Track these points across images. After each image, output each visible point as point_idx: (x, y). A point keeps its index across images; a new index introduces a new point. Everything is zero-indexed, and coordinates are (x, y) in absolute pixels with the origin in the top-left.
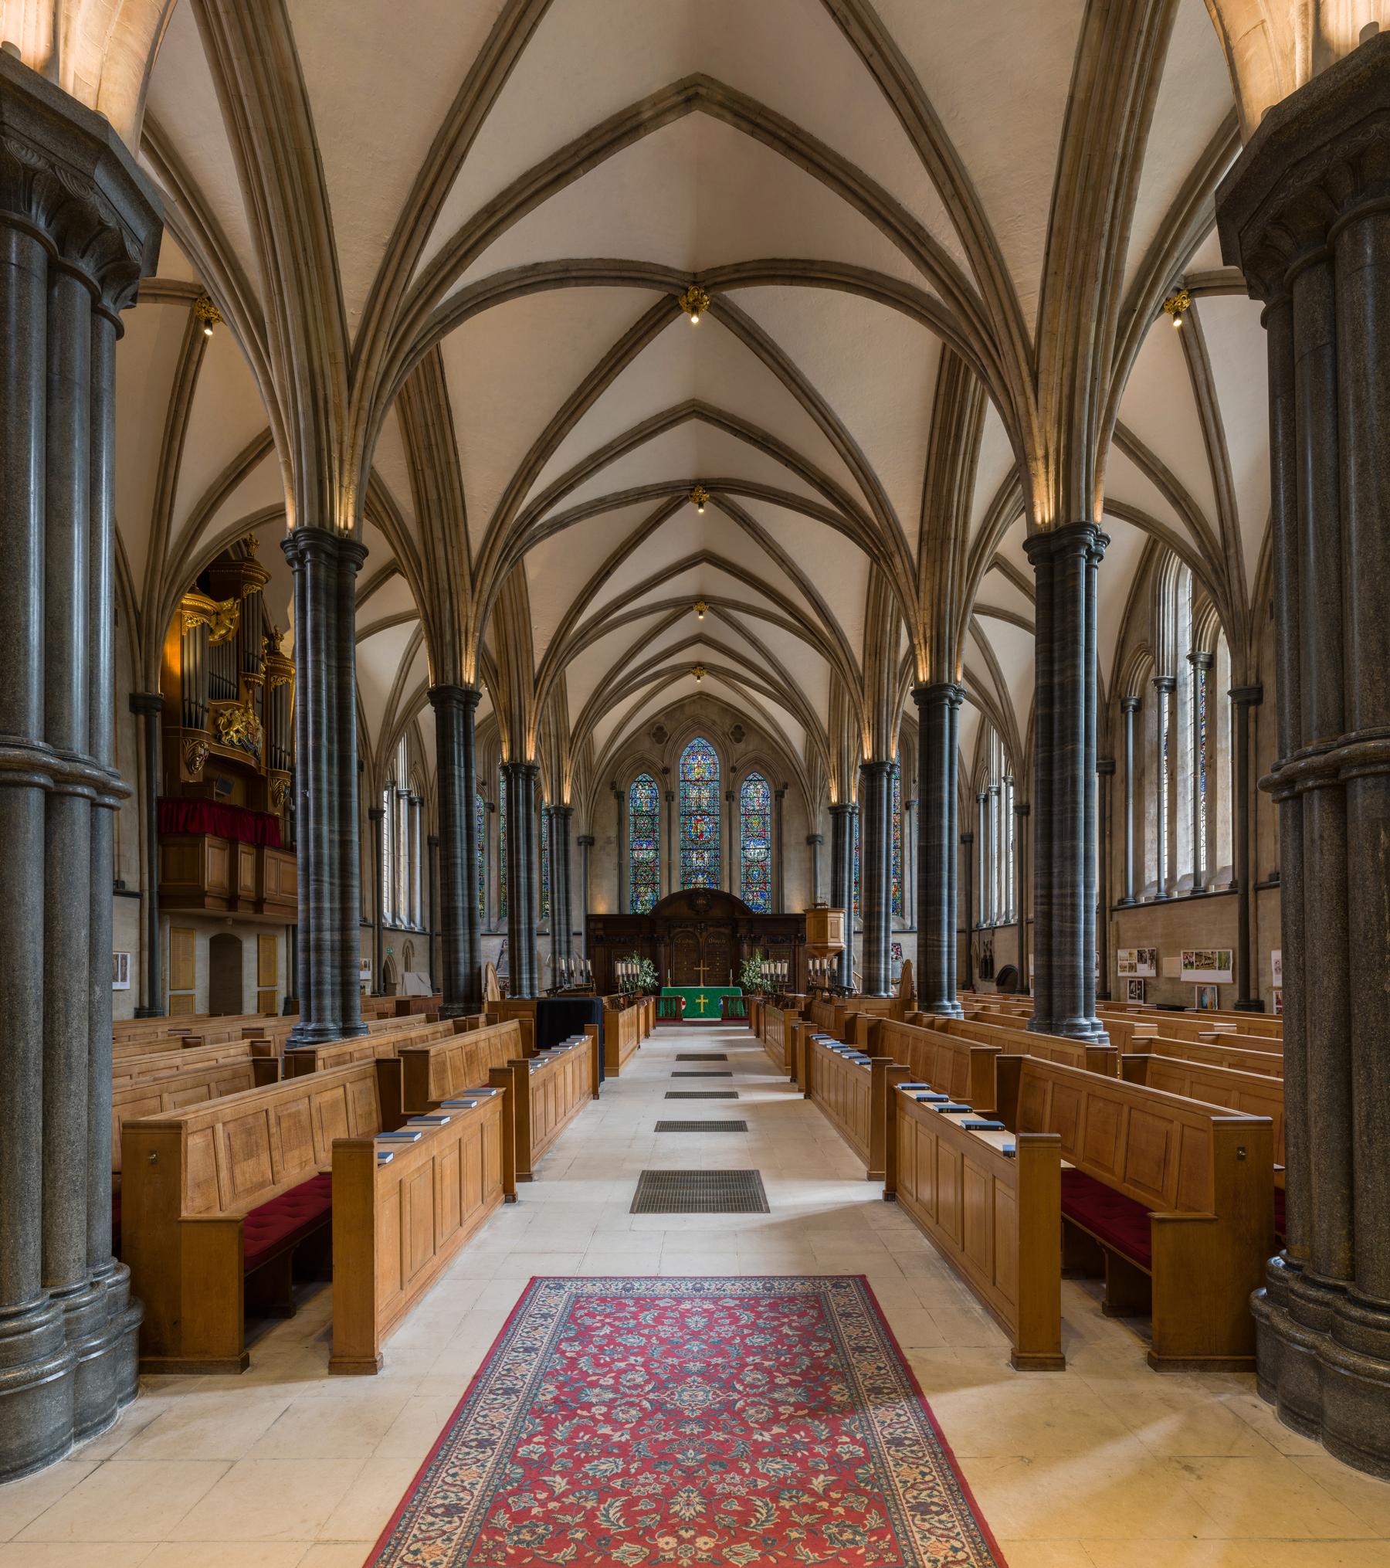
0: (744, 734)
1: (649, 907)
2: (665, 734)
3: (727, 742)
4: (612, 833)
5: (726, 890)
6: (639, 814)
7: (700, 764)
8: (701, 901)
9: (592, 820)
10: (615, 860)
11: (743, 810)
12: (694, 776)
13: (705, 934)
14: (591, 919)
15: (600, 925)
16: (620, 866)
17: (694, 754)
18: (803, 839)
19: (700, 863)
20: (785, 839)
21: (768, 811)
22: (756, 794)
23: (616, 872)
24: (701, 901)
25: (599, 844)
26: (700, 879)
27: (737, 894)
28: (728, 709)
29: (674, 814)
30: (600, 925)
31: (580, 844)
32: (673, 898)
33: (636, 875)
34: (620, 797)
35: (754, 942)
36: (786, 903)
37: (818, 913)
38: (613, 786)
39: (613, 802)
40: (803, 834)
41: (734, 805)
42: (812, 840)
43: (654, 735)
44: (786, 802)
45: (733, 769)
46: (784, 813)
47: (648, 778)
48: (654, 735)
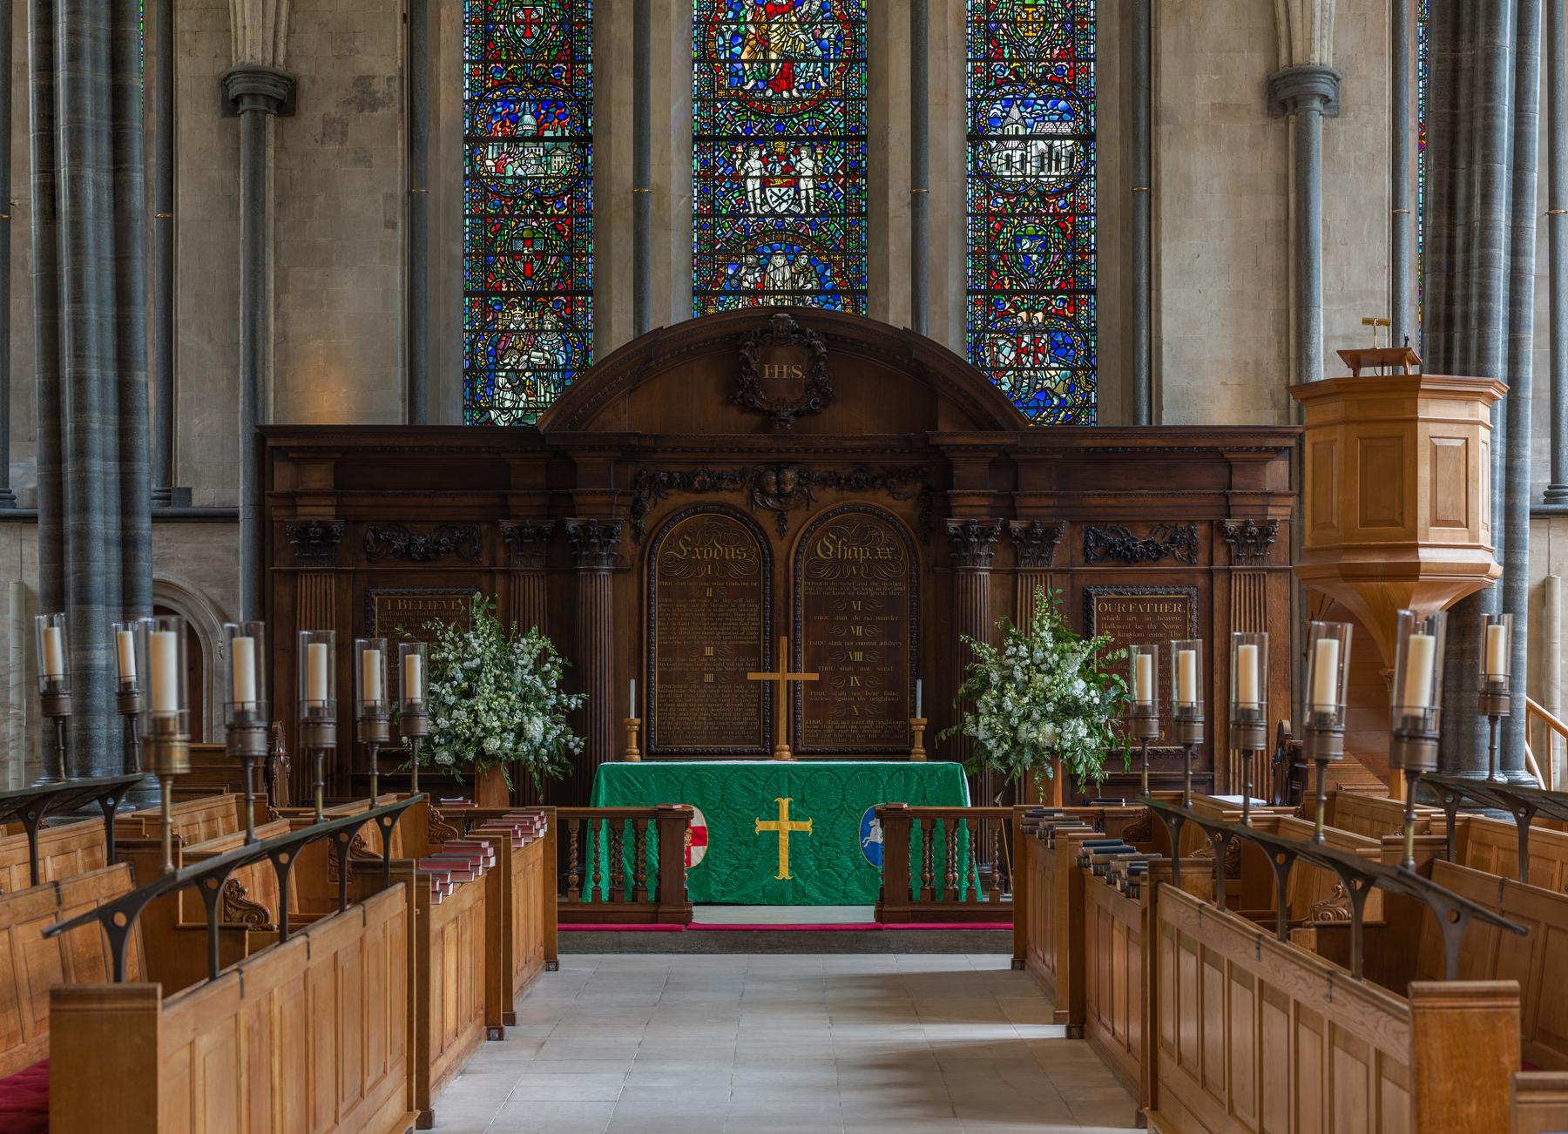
1: (546, 395)
4: (382, 60)
5: (897, 315)
8: (784, 370)
16: (415, 206)
18: (1248, 93)
19: (778, 199)
23: (399, 236)
24: (784, 370)
25: (318, 107)
26: (780, 271)
27: (952, 339)
30: (318, 477)
31: (231, 106)
36: (1172, 377)
40: (1250, 67)
42: (1289, 94)
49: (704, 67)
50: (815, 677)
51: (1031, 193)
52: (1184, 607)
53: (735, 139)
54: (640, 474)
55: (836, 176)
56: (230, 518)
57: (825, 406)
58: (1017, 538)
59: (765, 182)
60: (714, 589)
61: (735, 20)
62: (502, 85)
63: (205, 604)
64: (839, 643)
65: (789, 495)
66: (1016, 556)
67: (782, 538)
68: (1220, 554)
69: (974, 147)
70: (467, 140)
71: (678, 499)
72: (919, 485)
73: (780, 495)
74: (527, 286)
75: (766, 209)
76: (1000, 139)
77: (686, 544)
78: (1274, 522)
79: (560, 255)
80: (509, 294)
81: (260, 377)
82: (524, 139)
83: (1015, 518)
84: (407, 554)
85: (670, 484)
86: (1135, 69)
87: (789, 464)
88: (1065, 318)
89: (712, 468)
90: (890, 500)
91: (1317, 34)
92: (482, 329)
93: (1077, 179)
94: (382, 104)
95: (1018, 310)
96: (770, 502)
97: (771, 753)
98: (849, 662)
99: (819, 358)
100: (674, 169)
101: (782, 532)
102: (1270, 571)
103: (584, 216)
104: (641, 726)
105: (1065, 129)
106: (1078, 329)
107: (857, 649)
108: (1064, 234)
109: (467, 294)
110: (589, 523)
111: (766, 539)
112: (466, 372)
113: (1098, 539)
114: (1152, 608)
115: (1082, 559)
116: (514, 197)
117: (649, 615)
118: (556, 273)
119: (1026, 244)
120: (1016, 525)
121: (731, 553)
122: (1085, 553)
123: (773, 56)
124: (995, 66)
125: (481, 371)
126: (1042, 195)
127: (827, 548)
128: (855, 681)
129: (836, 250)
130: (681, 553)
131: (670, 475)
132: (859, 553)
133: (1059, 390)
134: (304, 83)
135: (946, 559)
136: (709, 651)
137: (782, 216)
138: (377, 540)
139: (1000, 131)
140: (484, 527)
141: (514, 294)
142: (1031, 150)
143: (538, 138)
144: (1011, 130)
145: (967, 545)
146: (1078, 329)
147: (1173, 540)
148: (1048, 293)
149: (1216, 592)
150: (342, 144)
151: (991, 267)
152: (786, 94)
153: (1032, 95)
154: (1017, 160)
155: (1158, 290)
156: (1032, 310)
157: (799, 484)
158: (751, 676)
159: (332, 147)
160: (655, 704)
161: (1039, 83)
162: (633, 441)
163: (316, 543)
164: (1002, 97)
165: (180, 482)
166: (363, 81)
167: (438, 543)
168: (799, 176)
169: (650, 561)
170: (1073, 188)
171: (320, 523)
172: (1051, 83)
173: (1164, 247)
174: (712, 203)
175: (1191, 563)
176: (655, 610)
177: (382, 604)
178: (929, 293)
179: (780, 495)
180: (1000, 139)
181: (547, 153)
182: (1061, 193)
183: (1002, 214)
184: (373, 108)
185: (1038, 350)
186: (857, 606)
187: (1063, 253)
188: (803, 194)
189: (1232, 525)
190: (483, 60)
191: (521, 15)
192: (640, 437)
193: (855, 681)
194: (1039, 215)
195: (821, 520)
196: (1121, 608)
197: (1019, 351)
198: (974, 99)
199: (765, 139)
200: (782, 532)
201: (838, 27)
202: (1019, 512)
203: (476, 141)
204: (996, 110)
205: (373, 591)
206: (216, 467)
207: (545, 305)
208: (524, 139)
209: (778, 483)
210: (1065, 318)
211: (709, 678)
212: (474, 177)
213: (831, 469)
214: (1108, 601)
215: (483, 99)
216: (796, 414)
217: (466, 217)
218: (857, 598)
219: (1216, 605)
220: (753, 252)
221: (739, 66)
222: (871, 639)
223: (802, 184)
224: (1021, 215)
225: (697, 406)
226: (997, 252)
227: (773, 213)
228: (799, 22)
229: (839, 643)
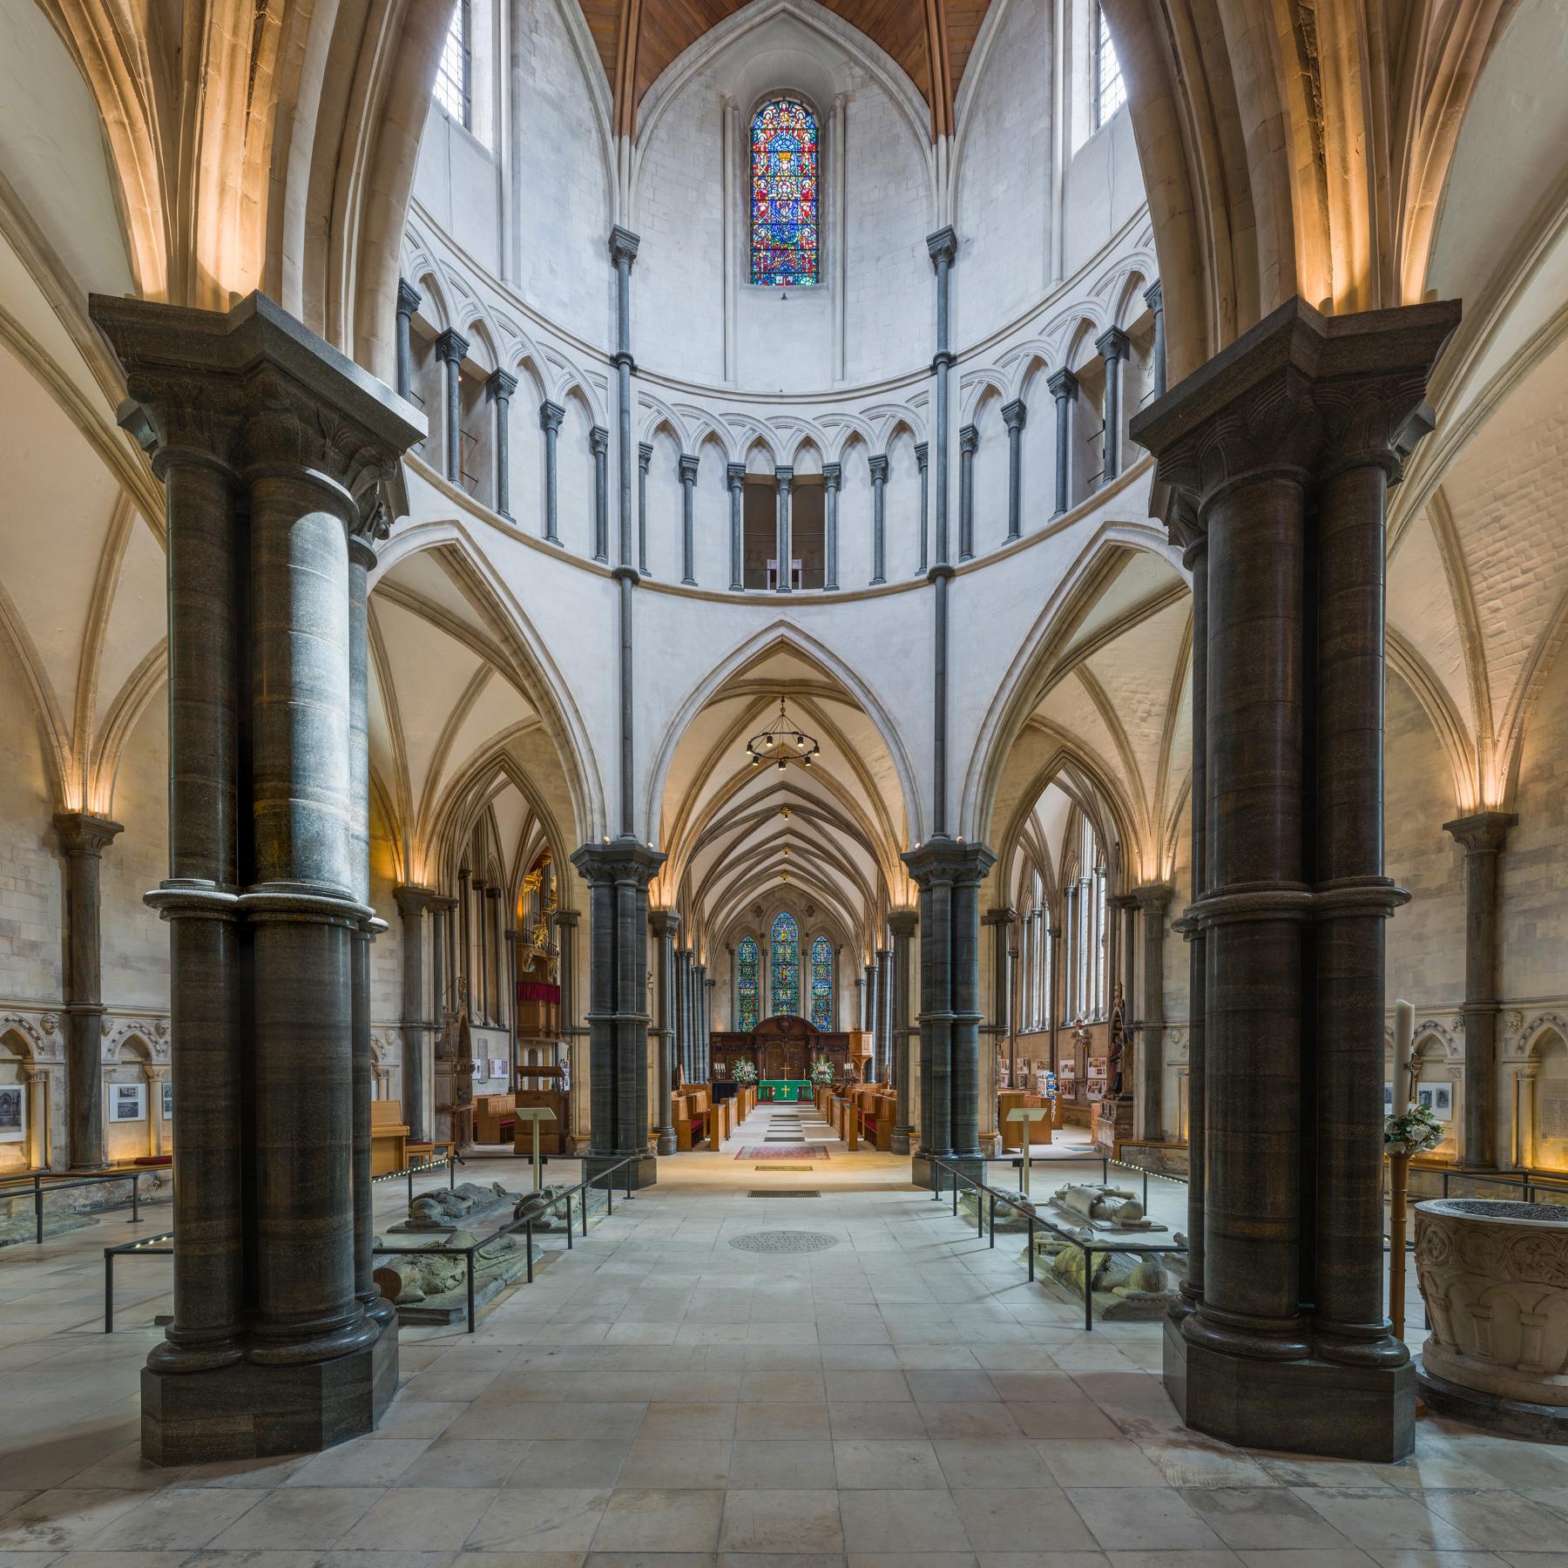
6: (743, 964)
7: (785, 932)
8: (786, 1024)
9: (715, 969)
12: (781, 938)
14: (712, 1035)
17: (780, 924)
22: (821, 950)
24: (786, 1024)
27: (809, 1020)
28: (803, 894)
32: (767, 1021)
34: (732, 953)
35: (820, 1050)
37: (857, 1033)
39: (728, 956)
100: (769, 994)
135: (808, 1051)
142: (822, 990)
154: (819, 991)
163: (719, 1049)
178: (807, 1011)
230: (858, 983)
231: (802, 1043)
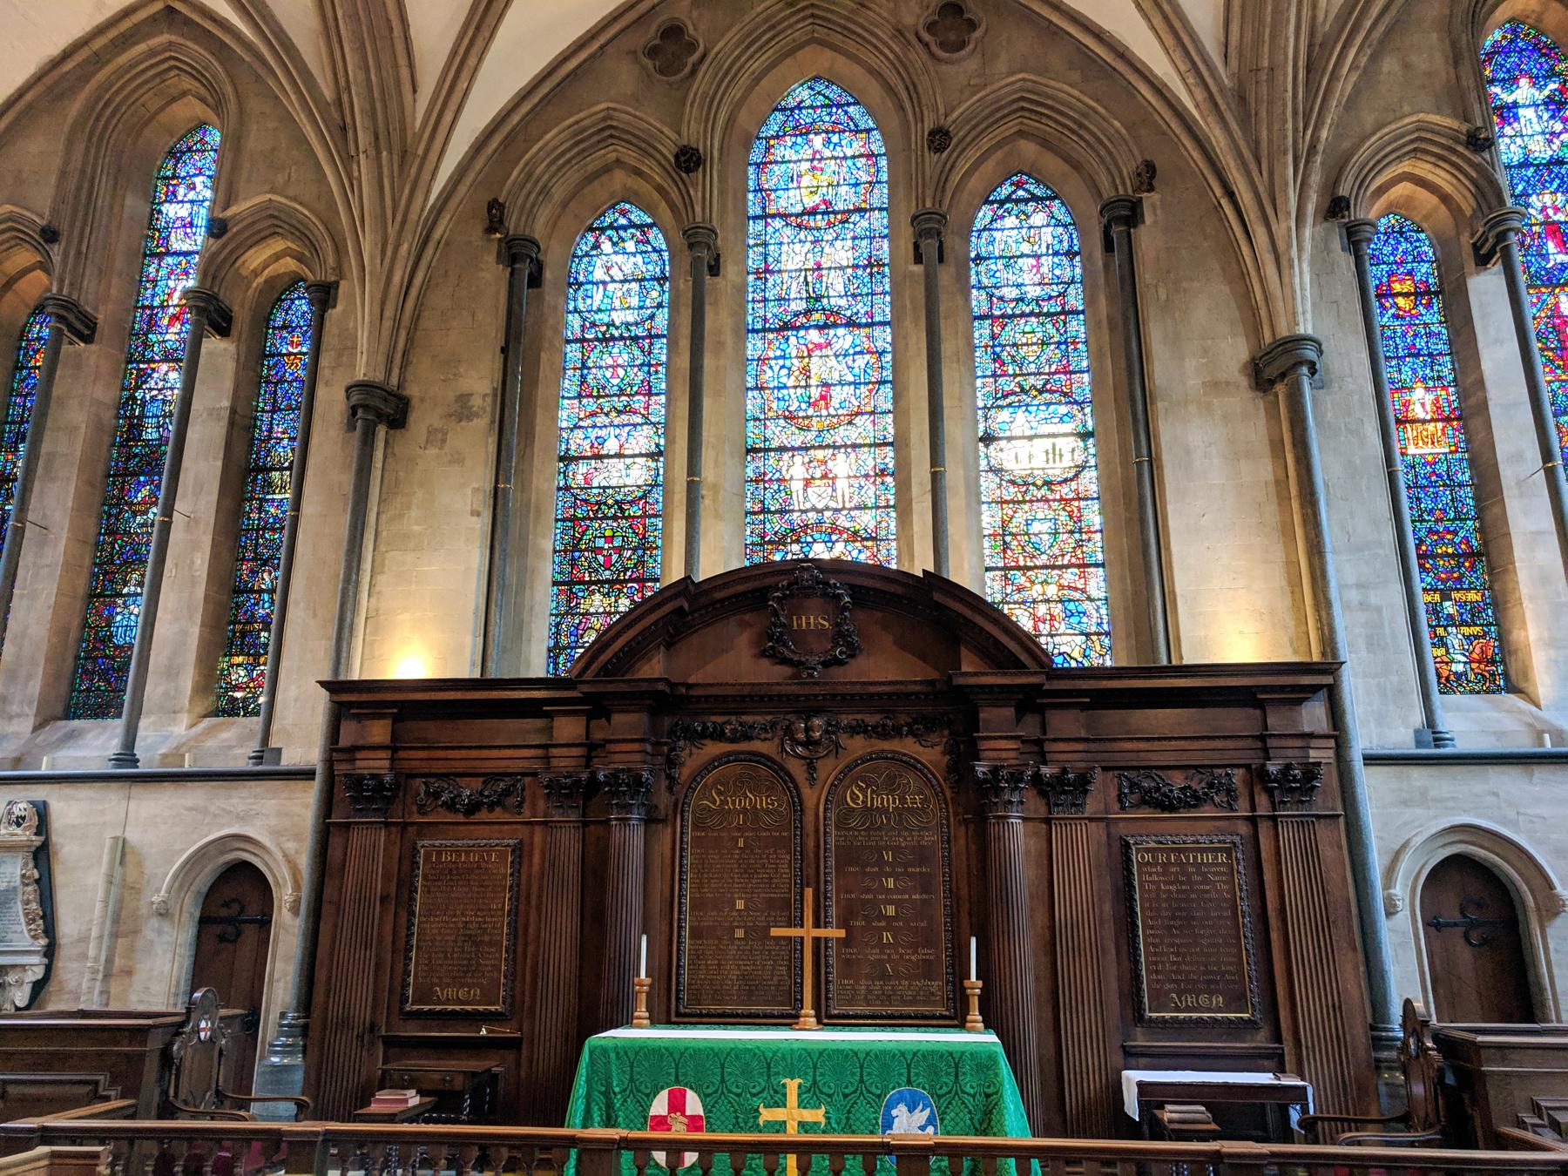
0: (973, 26)
2: (692, 46)
3: (918, 57)
4: (480, 381)
8: (814, 620)
9: (406, 335)
10: (489, 486)
11: (978, 302)
13: (828, 768)
14: (352, 700)
15: (379, 731)
19: (818, 496)
20: (1161, 369)
21: (1075, 299)
22: (1025, 248)
23: (482, 525)
29: (717, 320)
33: (572, 549)
38: (495, 215)
40: (1235, 351)
41: (945, 276)
43: (653, 52)
44: (1148, 239)
45: (939, 139)
46: (1146, 275)
47: (638, 216)
48: (653, 52)
49: (756, 393)
50: (842, 933)
51: (1039, 483)
52: (1229, 857)
53: (782, 449)
54: (677, 724)
55: (867, 476)
56: (308, 775)
57: (852, 656)
58: (1048, 784)
59: (808, 483)
60: (746, 839)
61: (784, 357)
62: (593, 414)
63: (279, 856)
64: (870, 896)
65: (817, 743)
66: (1048, 804)
67: (812, 786)
68: (1262, 801)
69: (987, 446)
70: (561, 459)
71: (714, 749)
72: (946, 732)
73: (809, 743)
74: (607, 575)
75: (808, 505)
76: (1010, 439)
77: (720, 793)
78: (1319, 764)
79: (635, 550)
80: (591, 583)
81: (345, 645)
82: (608, 456)
83: (1045, 763)
84: (451, 806)
85: (704, 735)
86: (1129, 359)
87: (818, 712)
88: (1076, 589)
89: (744, 718)
90: (918, 747)
91: (1300, 310)
92: (567, 613)
93: (1082, 468)
94: (477, 415)
95: (1032, 583)
96: (799, 750)
97: (790, 1019)
98: (881, 917)
99: (845, 608)
101: (812, 780)
102: (1318, 817)
103: (655, 516)
104: (651, 986)
105: (1068, 427)
106: (1089, 599)
107: (891, 902)
108: (1071, 517)
109: (555, 583)
110: (618, 770)
111: (796, 788)
112: (549, 650)
113: (1133, 786)
114: (1195, 858)
115: (1117, 806)
116: (597, 503)
117: (681, 866)
118: (630, 564)
119: (1035, 527)
120: (1046, 771)
121: (763, 802)
122: (1120, 801)
123: (813, 382)
124: (1001, 380)
125: (565, 648)
126: (1048, 483)
127: (856, 796)
128: (887, 937)
129: (866, 539)
130: (714, 802)
131: (705, 728)
132: (889, 802)
133: (1076, 654)
134: (415, 402)
136: (740, 905)
137: (821, 511)
138: (427, 793)
139: (1008, 434)
140: (528, 780)
141: (594, 583)
143: (619, 456)
144: (1017, 432)
145: (998, 791)
146: (1089, 599)
147: (1211, 785)
148: (1061, 567)
149: (1262, 840)
150: (441, 448)
151: (1006, 547)
152: (824, 413)
153: (1035, 402)
155: (1168, 549)
156: (1045, 582)
157: (827, 732)
158: (775, 932)
159: (432, 451)
160: (685, 961)
161: (1041, 392)
162: (661, 687)
164: (1010, 405)
165: (274, 743)
166: (464, 398)
167: (481, 794)
168: (834, 479)
169: (683, 811)
170: (1076, 476)
171: (373, 776)
172: (1051, 392)
173: (1170, 508)
174: (762, 502)
175: (1232, 810)
176: (688, 861)
177: (428, 856)
179: (809, 743)
180: (1010, 439)
181: (628, 467)
182: (1066, 481)
183: (1013, 501)
184: (469, 419)
185: (1053, 618)
186: (888, 856)
187: (1071, 532)
188: (839, 493)
189: (1273, 768)
190: (579, 396)
191: (610, 361)
192: (673, 686)
193: (887, 937)
194: (1047, 501)
195: (850, 768)
196: (1162, 858)
197: (1034, 617)
198: (985, 407)
199: (807, 449)
200: (812, 780)
201: (867, 357)
202: (1048, 757)
203: (567, 459)
204: (1004, 415)
205: (420, 843)
206: (302, 728)
207: (620, 591)
208: (608, 456)
209: (807, 730)
210: (1076, 589)
211: (740, 933)
212: (567, 488)
213: (859, 717)
214: (1148, 850)
215: (576, 427)
216: (826, 664)
217: (557, 520)
218: (887, 848)
219: (1264, 855)
220: (798, 541)
221: (785, 392)
222: (904, 892)
223: (841, 484)
224: (1031, 501)
225: (734, 660)
226: (1011, 534)
227: (814, 509)
228: (836, 356)
229: (870, 896)
230: (1279, 368)
231: (930, 753)
